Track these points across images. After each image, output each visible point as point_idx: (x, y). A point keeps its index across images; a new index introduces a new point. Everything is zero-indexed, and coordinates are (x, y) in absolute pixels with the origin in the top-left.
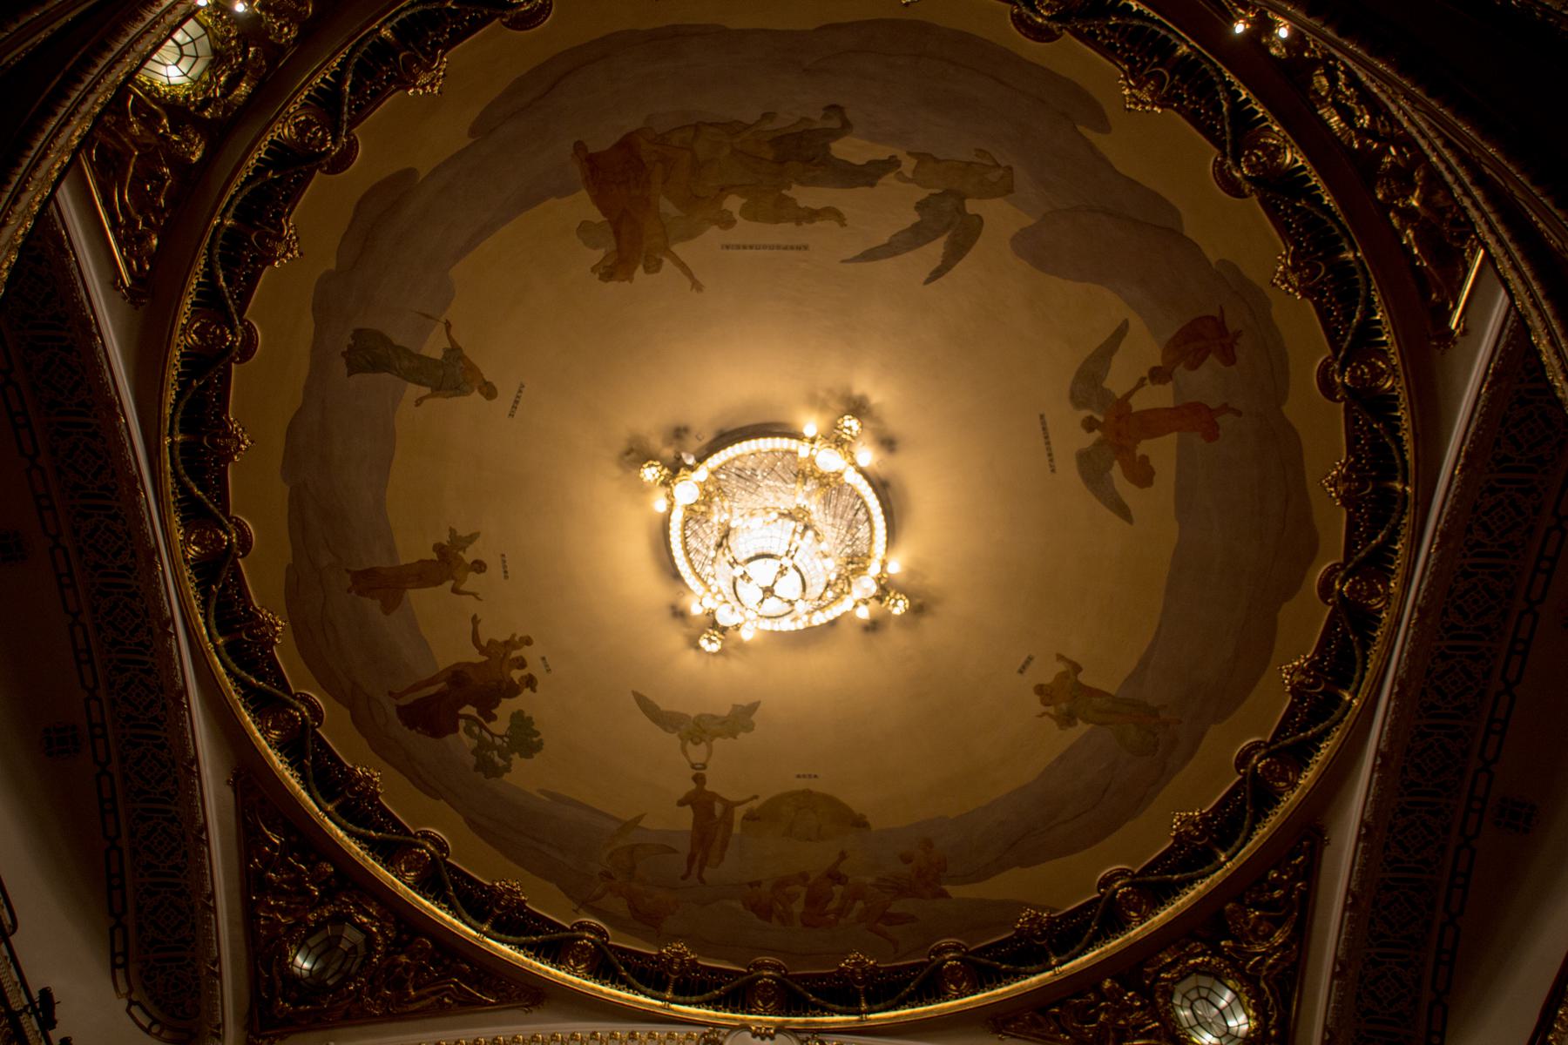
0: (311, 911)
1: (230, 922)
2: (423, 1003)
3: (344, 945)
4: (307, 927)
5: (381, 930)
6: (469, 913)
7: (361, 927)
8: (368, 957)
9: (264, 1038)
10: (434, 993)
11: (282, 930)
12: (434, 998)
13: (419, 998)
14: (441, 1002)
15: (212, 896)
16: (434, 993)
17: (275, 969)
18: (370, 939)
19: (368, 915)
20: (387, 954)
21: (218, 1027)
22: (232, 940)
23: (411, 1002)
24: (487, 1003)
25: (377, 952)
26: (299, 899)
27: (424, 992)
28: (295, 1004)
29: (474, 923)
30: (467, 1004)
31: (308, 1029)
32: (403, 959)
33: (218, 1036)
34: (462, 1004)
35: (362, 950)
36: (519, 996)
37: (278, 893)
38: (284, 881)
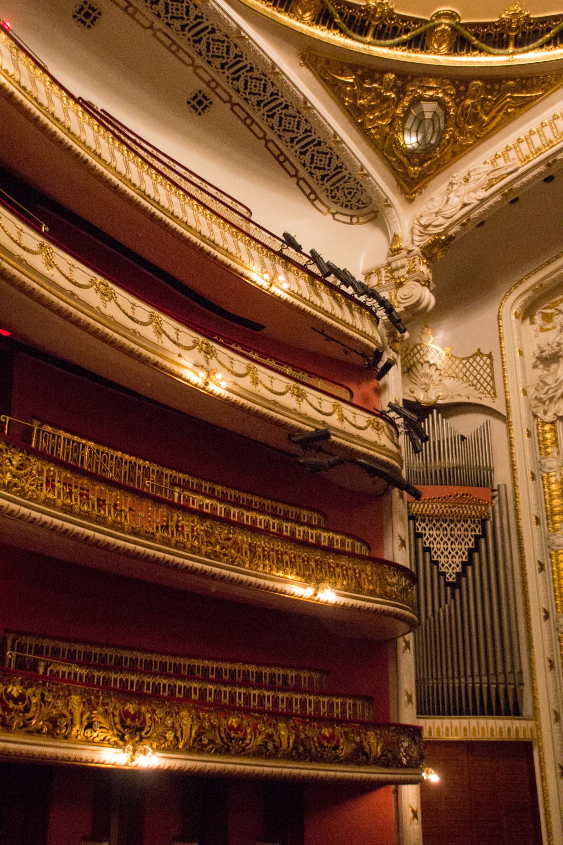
0: (396, 107)
1: (356, 142)
2: (496, 120)
3: (428, 116)
4: (401, 119)
5: (444, 91)
6: (494, 46)
7: (431, 99)
8: (446, 114)
9: (415, 192)
10: (499, 111)
11: (387, 129)
12: (501, 114)
13: (492, 120)
14: (507, 114)
15: (336, 135)
16: (499, 111)
17: (397, 153)
18: (441, 103)
19: (432, 89)
20: (457, 104)
21: (386, 201)
22: (364, 152)
23: (488, 124)
24: (537, 97)
25: (450, 108)
26: (385, 105)
27: (493, 114)
28: (421, 164)
29: (501, 51)
30: (524, 105)
31: (435, 175)
32: (469, 102)
33: (389, 206)
34: (520, 107)
35: (440, 112)
36: (556, 80)
37: (371, 109)
38: (370, 101)
